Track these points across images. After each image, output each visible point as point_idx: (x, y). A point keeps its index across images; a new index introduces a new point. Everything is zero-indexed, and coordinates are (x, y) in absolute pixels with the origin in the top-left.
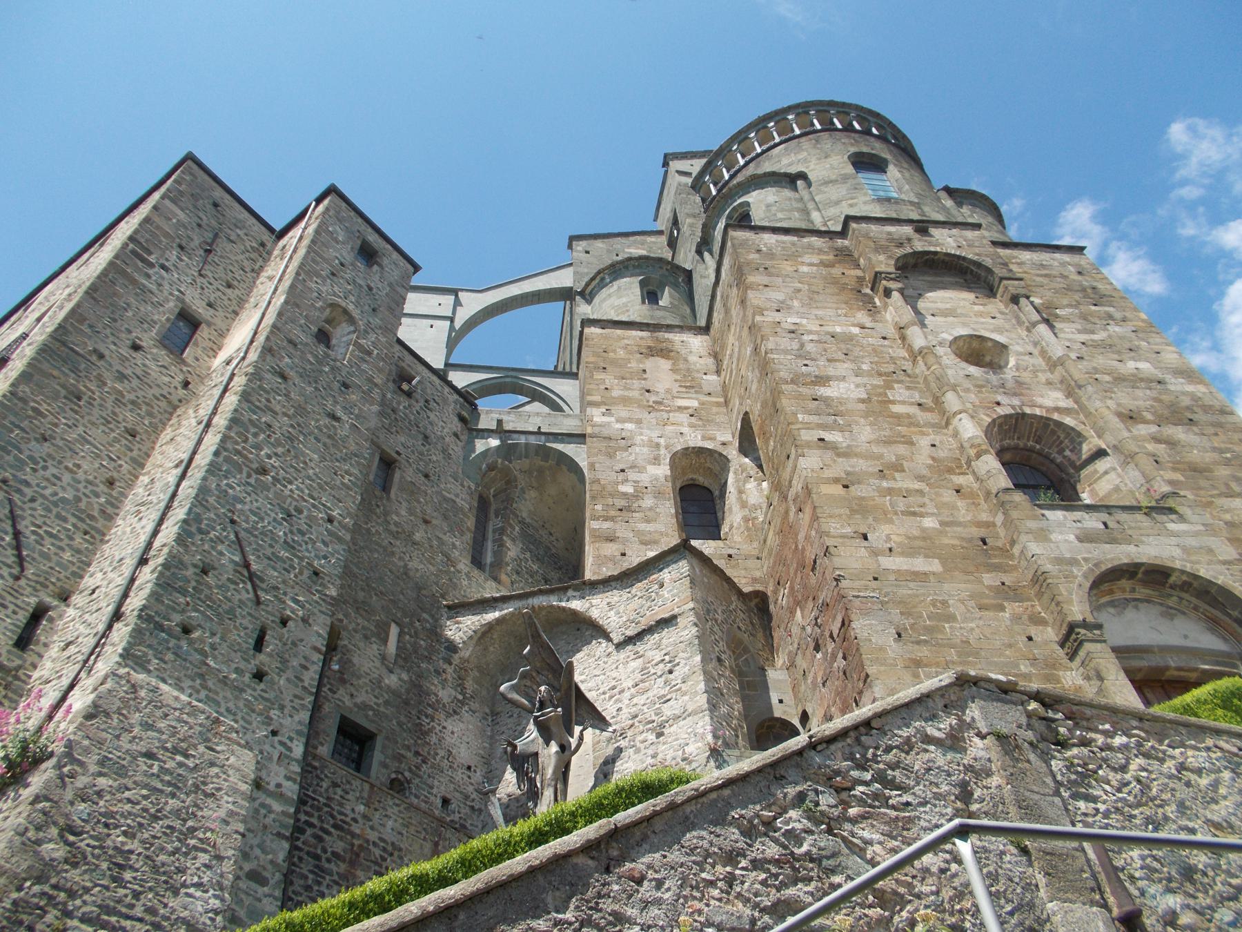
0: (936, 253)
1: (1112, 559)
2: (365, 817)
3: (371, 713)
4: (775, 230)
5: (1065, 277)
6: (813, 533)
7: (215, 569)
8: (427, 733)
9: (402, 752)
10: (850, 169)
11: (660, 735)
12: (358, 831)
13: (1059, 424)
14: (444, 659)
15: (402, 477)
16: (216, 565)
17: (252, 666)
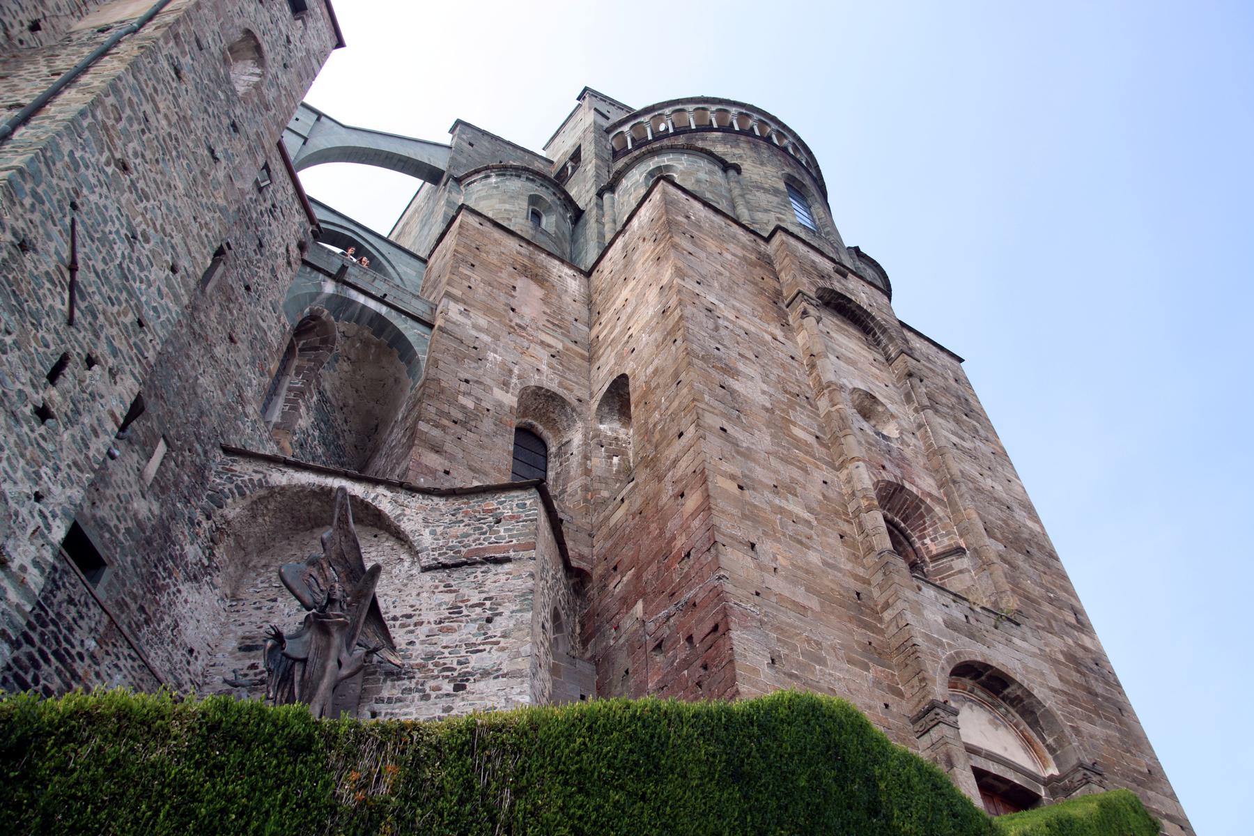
0: (850, 301)
1: (970, 653)
2: (92, 656)
3: (107, 535)
4: (706, 204)
5: (946, 379)
6: (696, 523)
7: (35, 251)
8: (159, 589)
9: (128, 599)
10: (782, 186)
11: (459, 687)
12: (80, 672)
13: (929, 510)
14: (203, 509)
15: (224, 275)
16: (39, 246)
17: (38, 398)
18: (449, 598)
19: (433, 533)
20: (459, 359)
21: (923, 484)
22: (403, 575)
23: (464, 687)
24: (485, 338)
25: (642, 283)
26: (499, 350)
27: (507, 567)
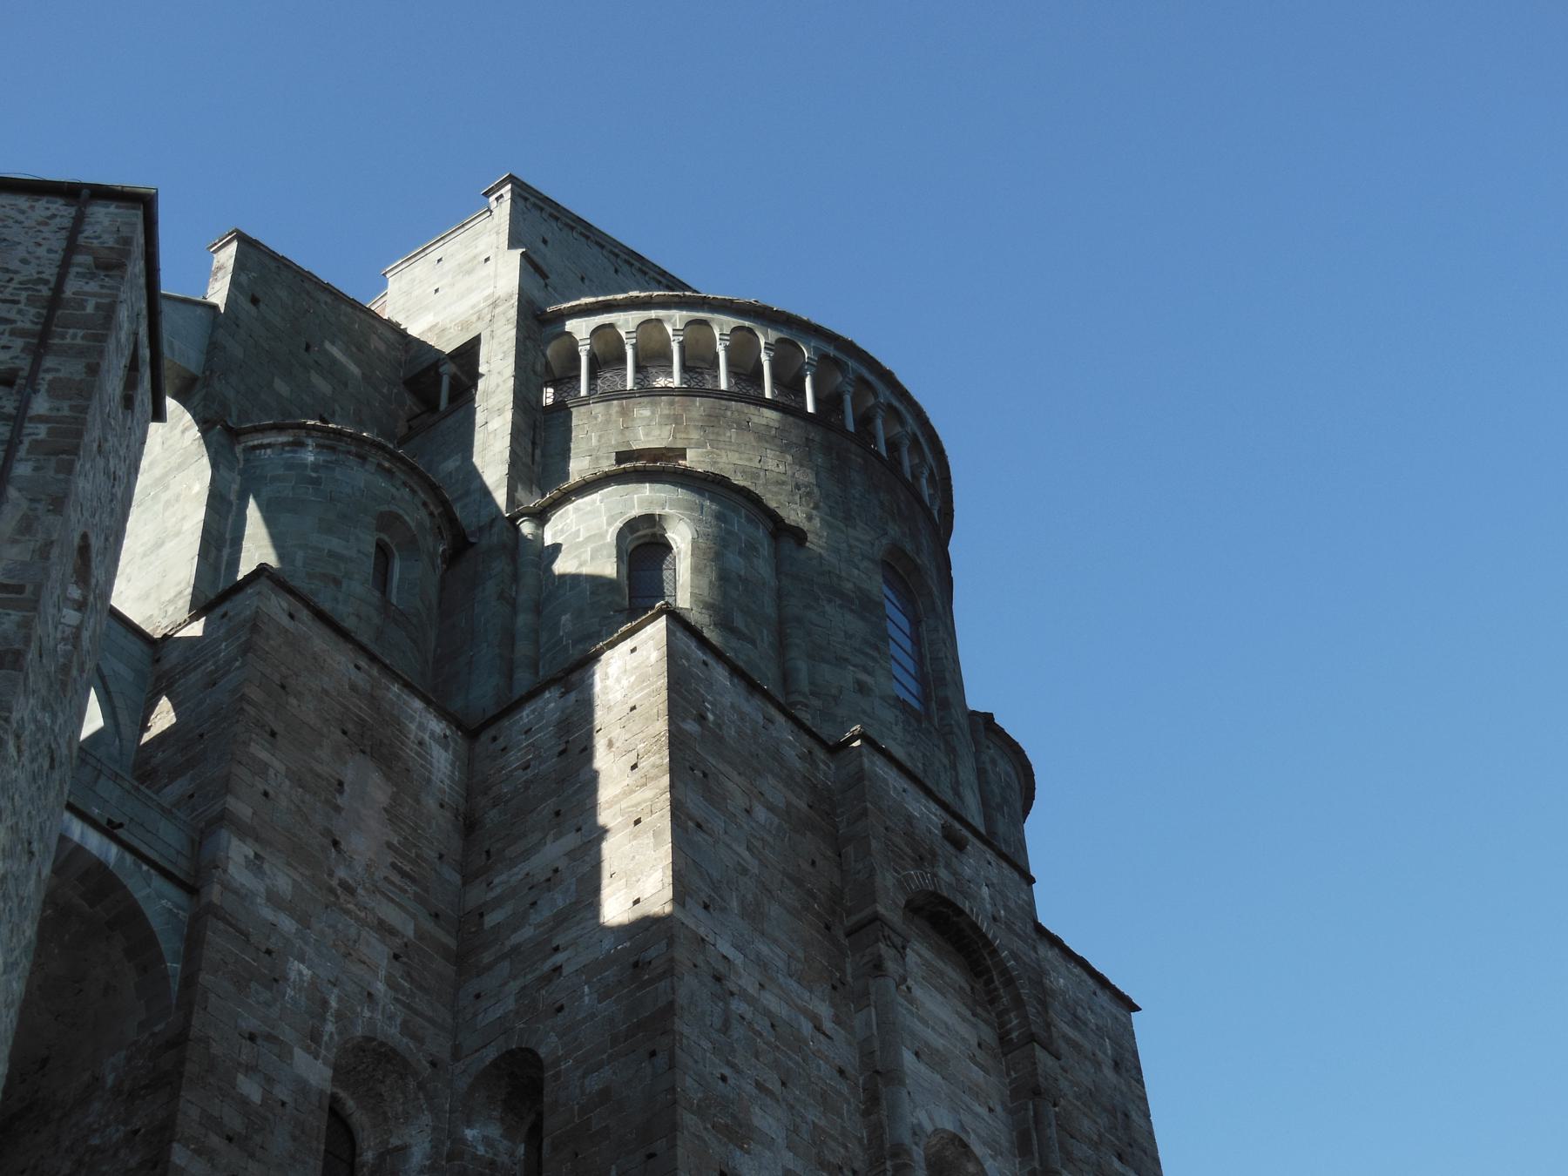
0: (960, 912)
4: (736, 671)
5: (1098, 1065)
10: (877, 585)
24: (288, 924)
26: (310, 952)
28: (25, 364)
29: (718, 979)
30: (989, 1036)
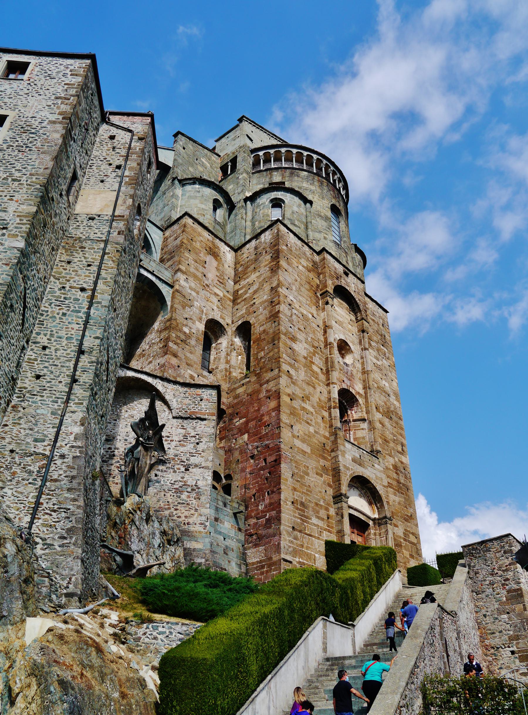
5: (378, 325)
6: (273, 414)
10: (329, 214)
11: (187, 470)
13: (357, 400)
18: (183, 431)
19: (177, 401)
20: (184, 308)
21: (357, 388)
22: (166, 418)
23: (188, 470)
24: (194, 294)
25: (262, 278)
26: (199, 300)
27: (205, 422)
28: (123, 163)
29: (290, 305)
30: (353, 318)
